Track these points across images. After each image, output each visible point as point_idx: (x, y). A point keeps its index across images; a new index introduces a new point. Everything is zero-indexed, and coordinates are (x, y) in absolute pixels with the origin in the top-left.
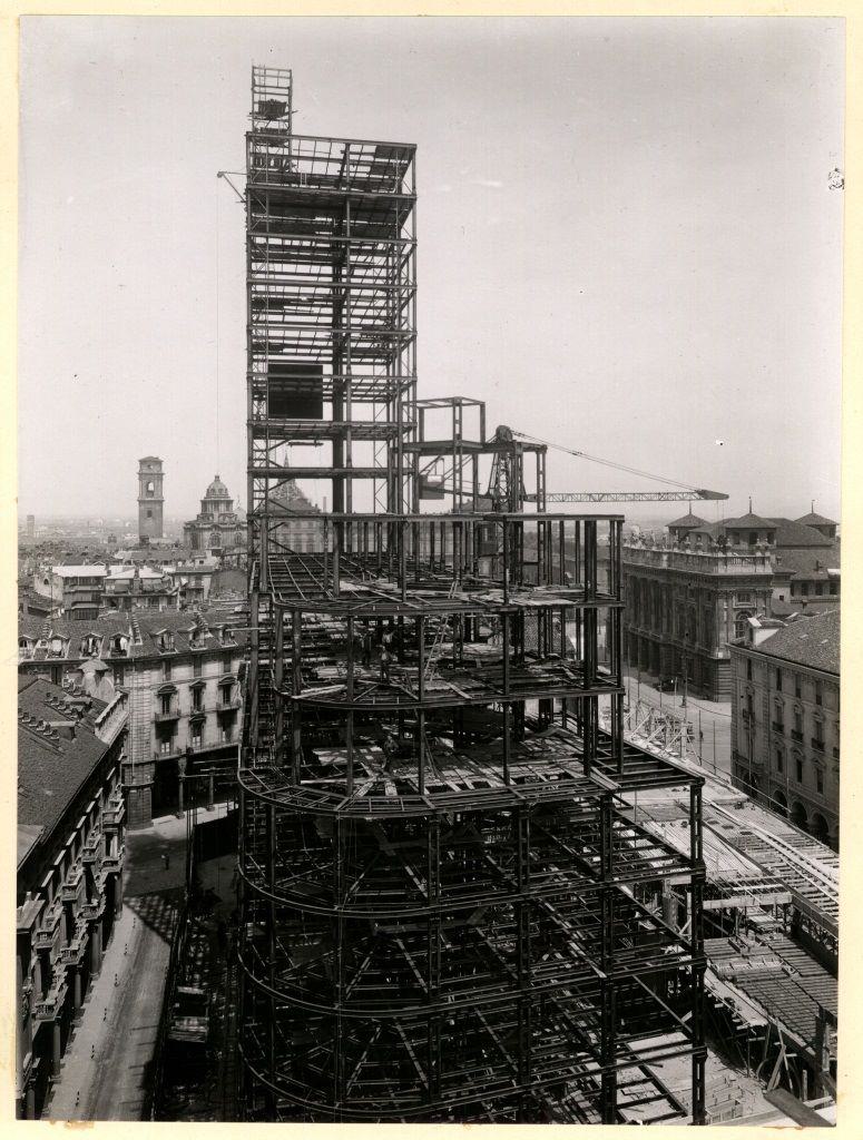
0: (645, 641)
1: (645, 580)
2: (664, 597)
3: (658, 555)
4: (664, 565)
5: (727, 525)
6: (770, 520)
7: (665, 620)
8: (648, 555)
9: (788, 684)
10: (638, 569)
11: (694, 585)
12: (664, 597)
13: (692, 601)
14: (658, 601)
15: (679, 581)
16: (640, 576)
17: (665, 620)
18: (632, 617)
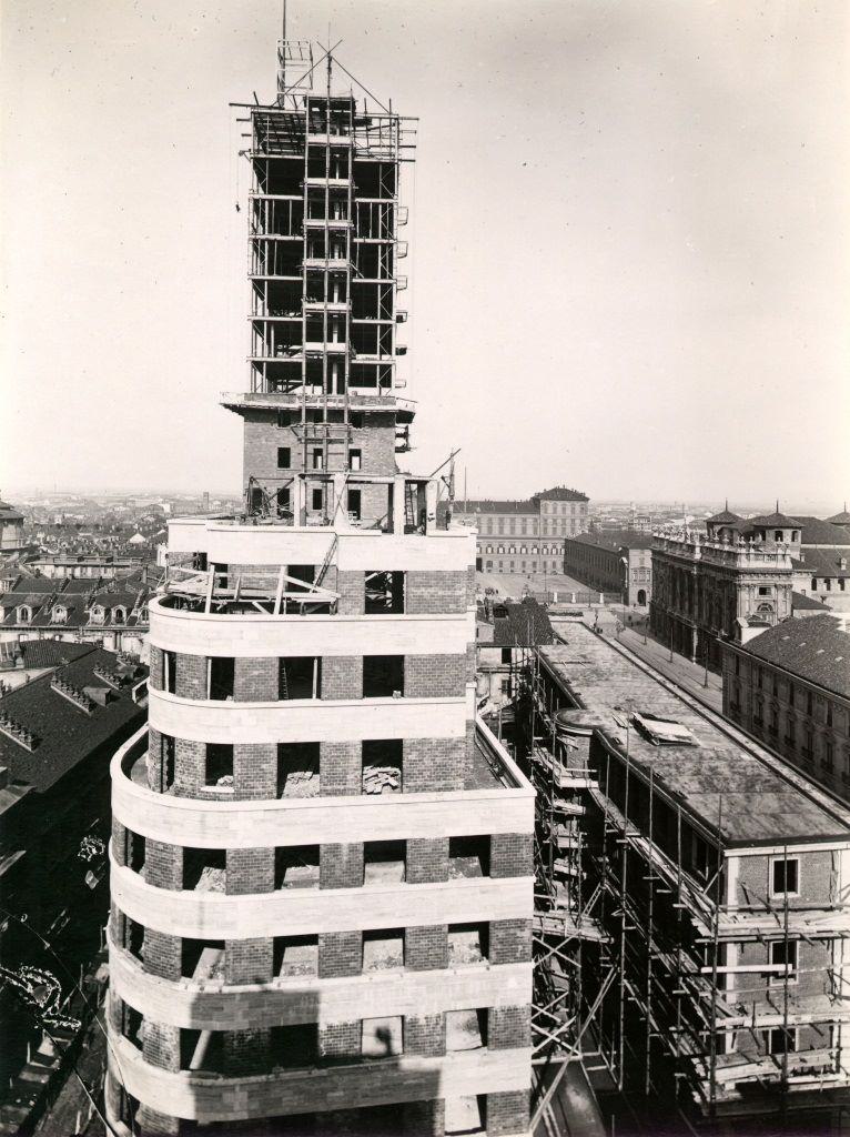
0: (680, 625)
1: (680, 569)
2: (696, 586)
3: (692, 548)
4: (698, 556)
5: (755, 523)
6: (795, 518)
7: (696, 607)
8: (684, 547)
9: (768, 682)
10: (675, 559)
11: (720, 577)
12: (696, 586)
13: (718, 591)
14: (691, 589)
15: (705, 571)
16: (677, 565)
17: (696, 607)
18: (670, 602)
